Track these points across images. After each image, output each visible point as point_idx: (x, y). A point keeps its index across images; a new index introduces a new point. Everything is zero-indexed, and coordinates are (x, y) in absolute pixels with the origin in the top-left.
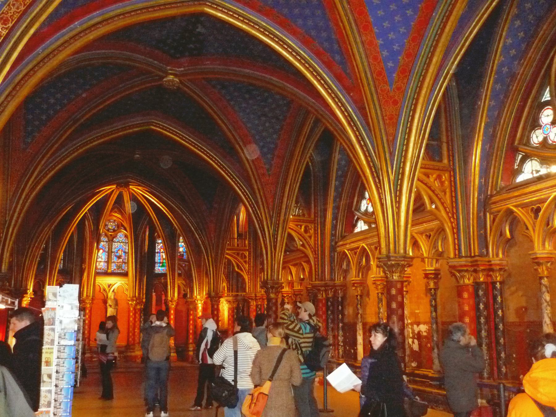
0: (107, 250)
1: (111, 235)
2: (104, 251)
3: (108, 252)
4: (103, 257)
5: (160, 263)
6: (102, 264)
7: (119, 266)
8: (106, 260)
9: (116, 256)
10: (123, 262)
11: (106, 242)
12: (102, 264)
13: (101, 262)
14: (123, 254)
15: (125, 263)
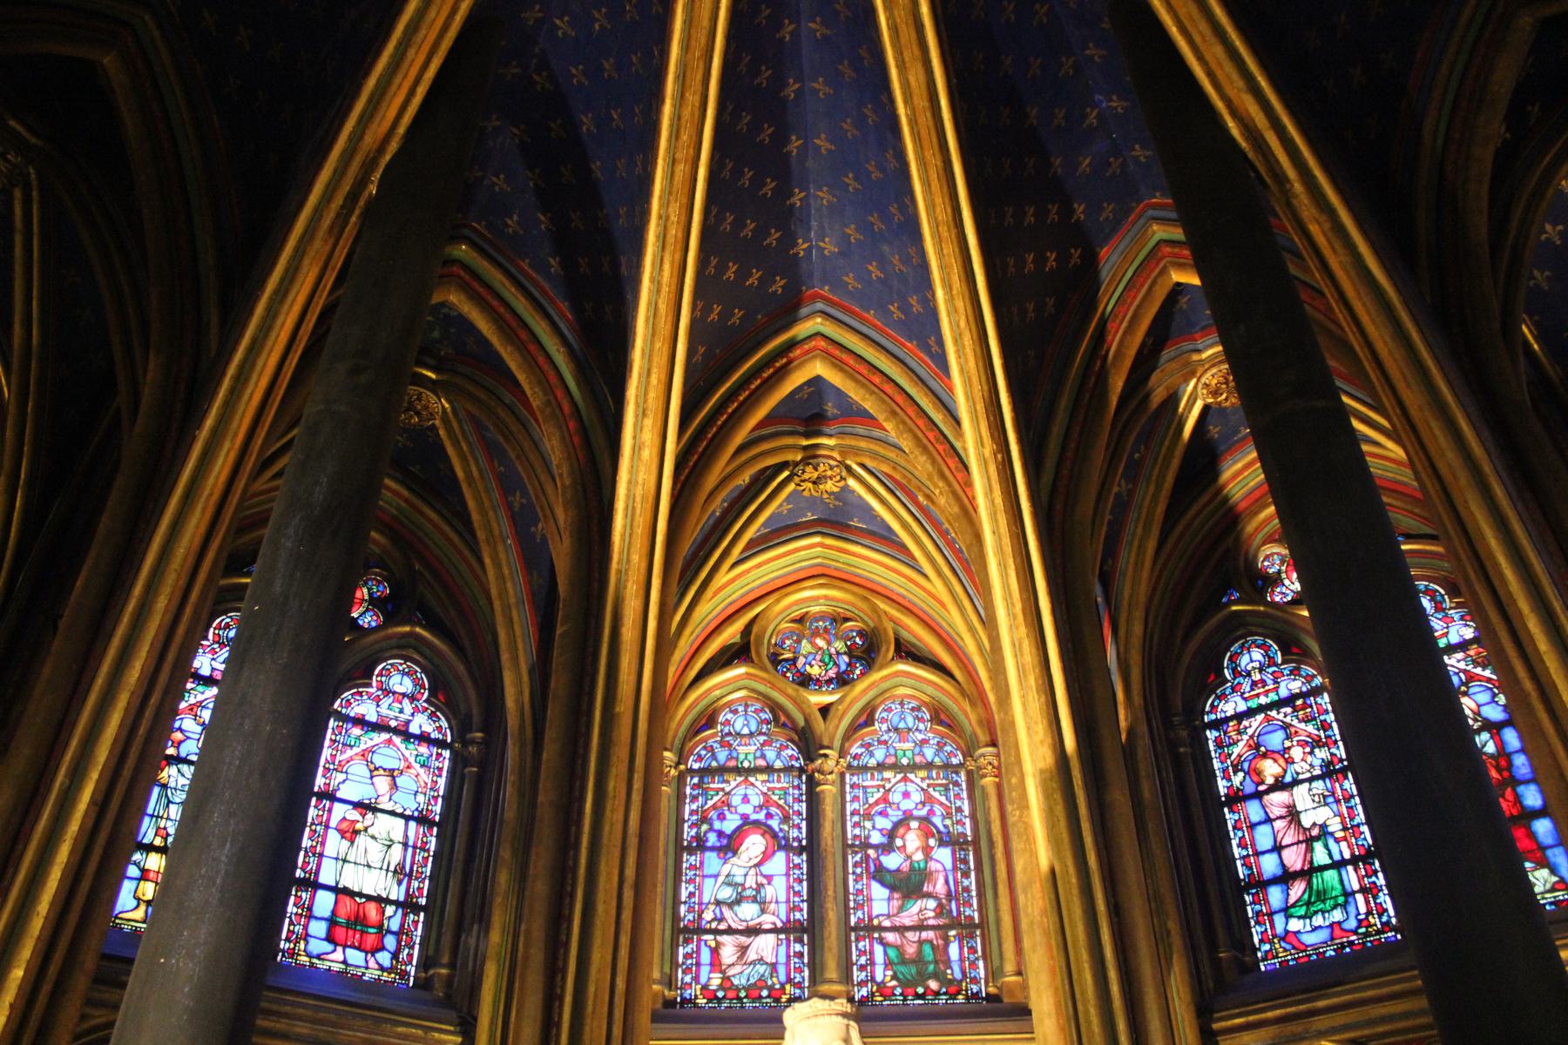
0: (799, 833)
1: (825, 710)
2: (778, 842)
3: (812, 848)
4: (777, 890)
5: (1286, 878)
6: (765, 946)
7: (918, 960)
8: (802, 916)
9: (879, 874)
10: (952, 923)
11: (787, 769)
12: (765, 946)
13: (753, 931)
14: (944, 855)
15: (967, 929)
